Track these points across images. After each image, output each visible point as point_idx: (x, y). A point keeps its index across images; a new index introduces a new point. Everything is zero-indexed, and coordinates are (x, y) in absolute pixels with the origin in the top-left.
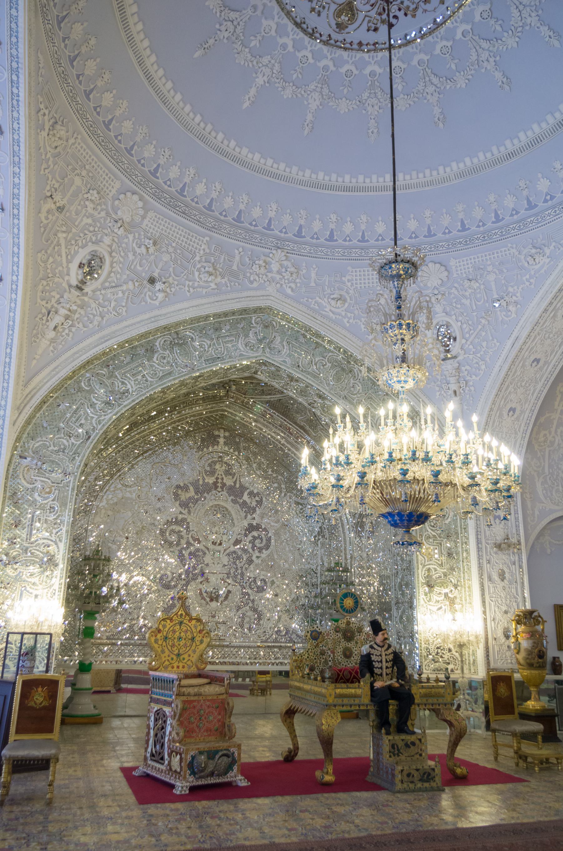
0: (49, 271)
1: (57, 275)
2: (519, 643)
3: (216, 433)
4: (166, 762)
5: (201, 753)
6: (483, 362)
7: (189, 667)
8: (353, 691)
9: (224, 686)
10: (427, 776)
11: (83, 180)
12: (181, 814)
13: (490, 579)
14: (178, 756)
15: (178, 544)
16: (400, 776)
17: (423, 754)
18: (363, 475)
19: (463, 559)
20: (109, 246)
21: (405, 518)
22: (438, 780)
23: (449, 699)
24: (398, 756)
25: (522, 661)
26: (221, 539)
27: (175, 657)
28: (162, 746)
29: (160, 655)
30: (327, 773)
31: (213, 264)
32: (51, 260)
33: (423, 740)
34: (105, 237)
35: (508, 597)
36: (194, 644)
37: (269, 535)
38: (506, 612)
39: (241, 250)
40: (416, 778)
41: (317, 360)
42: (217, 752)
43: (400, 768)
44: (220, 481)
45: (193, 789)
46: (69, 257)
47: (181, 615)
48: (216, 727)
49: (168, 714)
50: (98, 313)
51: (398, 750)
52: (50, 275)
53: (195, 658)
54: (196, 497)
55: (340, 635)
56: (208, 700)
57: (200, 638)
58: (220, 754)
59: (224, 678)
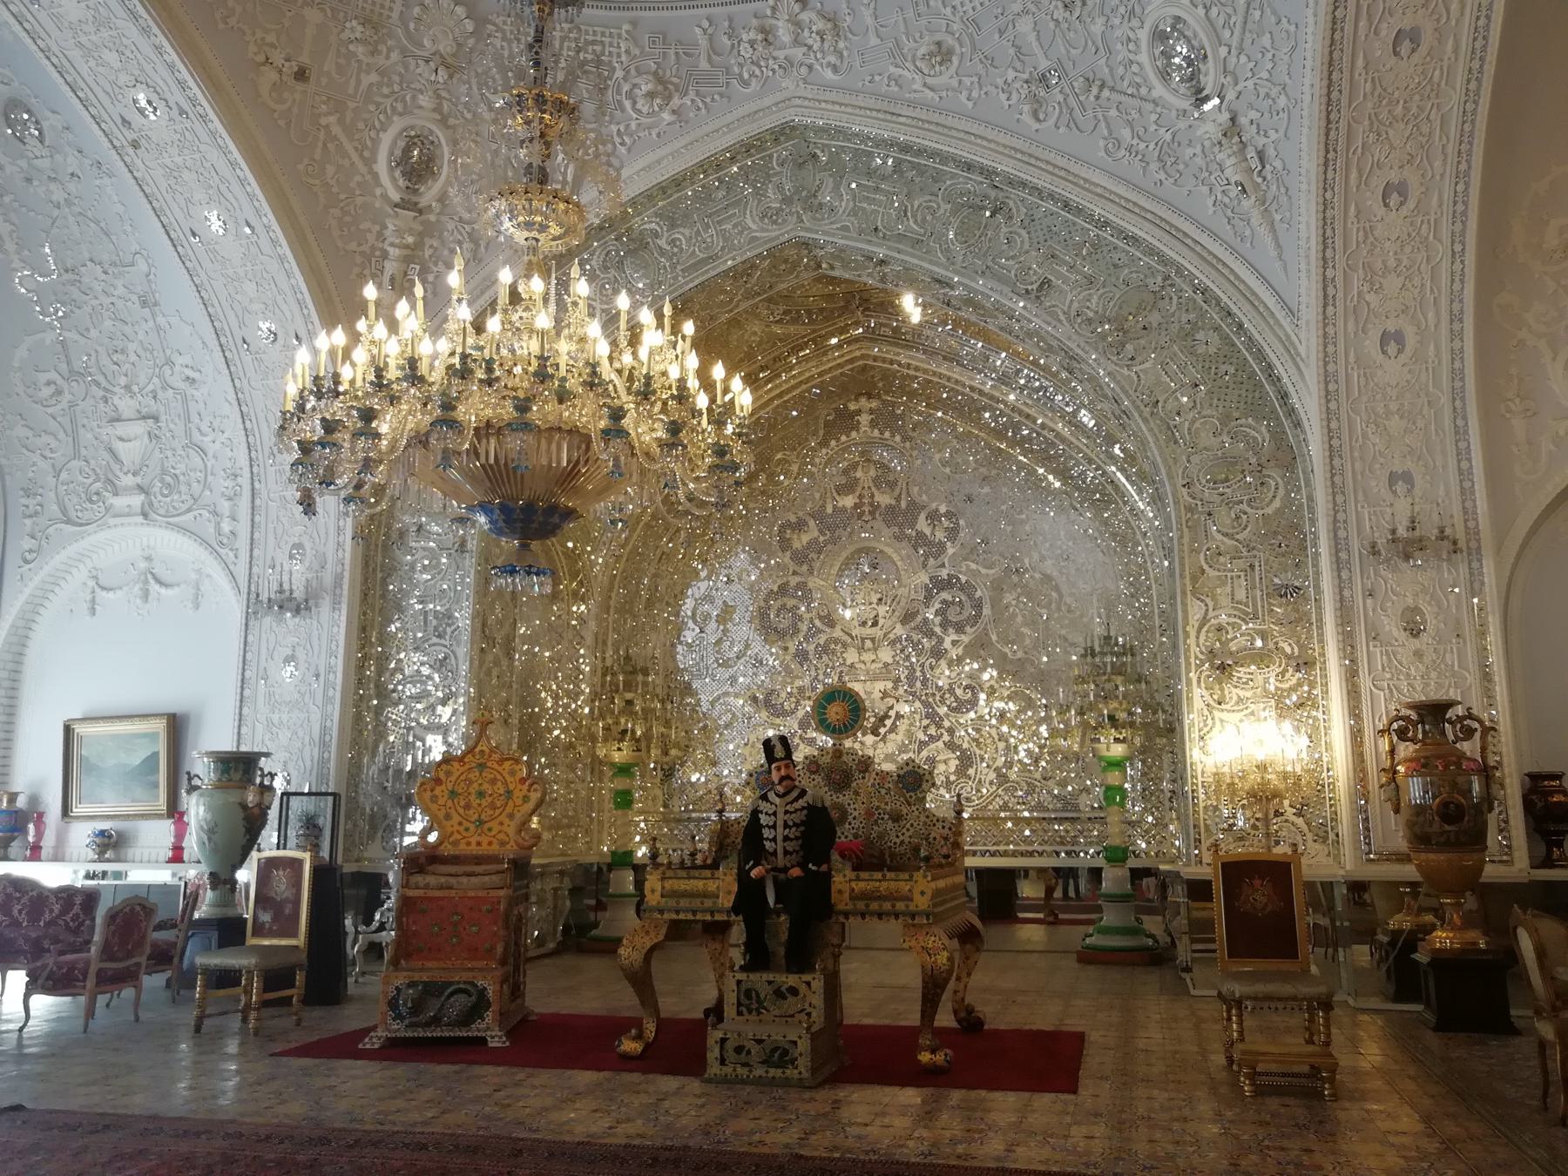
0: (335, 190)
1: (358, 192)
2: (1397, 786)
3: (852, 407)
5: (409, 985)
6: (1280, 88)
7: (503, 844)
8: (700, 884)
10: (780, 1056)
11: (323, 10)
13: (1374, 636)
17: (814, 1014)
20: (434, 110)
22: (803, 1067)
23: (922, 907)
24: (759, 1013)
26: (875, 613)
30: (639, 1037)
31: (655, 74)
32: (330, 170)
34: (421, 97)
35: (1434, 675)
36: (511, 803)
37: (978, 594)
39: (706, 24)
40: (755, 1057)
41: (916, 204)
42: (451, 983)
46: (366, 154)
48: (487, 946)
50: (466, 236)
52: (342, 196)
54: (822, 539)
57: (525, 792)
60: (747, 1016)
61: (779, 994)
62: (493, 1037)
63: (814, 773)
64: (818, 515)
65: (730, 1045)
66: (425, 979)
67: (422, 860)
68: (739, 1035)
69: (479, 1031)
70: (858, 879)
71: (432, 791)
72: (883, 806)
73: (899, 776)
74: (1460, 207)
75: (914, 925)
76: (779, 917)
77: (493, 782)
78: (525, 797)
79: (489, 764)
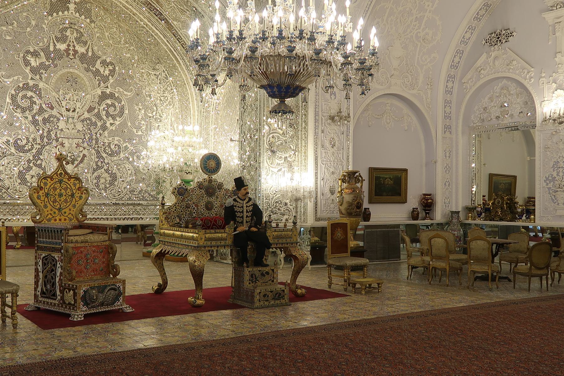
4: (59, 298)
7: (71, 220)
8: (220, 235)
9: (107, 234)
10: (278, 296)
12: (85, 333)
14: (72, 292)
15: (30, 109)
17: (275, 281)
18: (253, 50)
19: (302, 129)
21: (283, 89)
22: (287, 297)
23: (295, 240)
25: (344, 212)
27: (57, 212)
28: (54, 284)
29: (43, 210)
33: (275, 271)
35: (336, 161)
36: (74, 199)
37: (123, 103)
38: (333, 173)
42: (106, 287)
43: (258, 291)
44: (71, 48)
45: (86, 316)
49: (57, 259)
51: (256, 278)
53: (74, 211)
54: (47, 63)
55: (203, 191)
56: (94, 246)
57: (79, 195)
58: (109, 288)
59: (107, 228)
63: (201, 189)
64: (46, 50)
68: (266, 290)
69: (118, 306)
73: (232, 191)
74: (367, 9)
77: (66, 189)
79: (64, 180)
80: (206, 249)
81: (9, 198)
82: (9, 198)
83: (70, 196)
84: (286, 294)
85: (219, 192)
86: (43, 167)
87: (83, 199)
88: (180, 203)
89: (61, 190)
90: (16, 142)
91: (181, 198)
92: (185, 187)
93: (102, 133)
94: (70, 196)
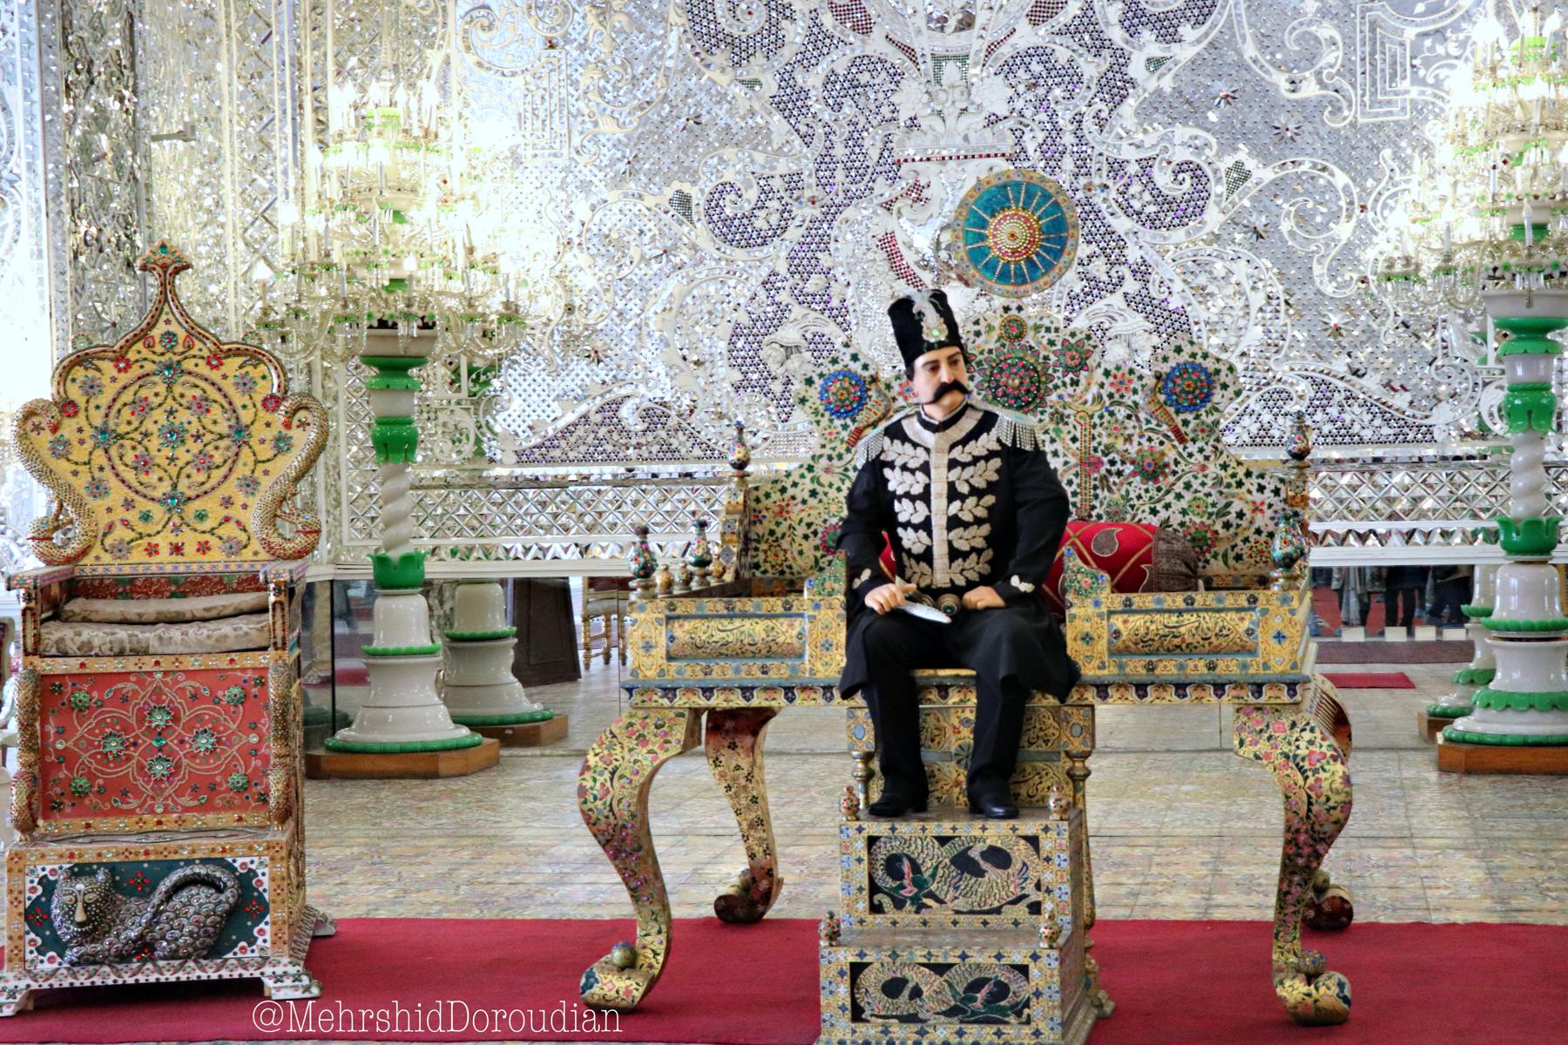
7: (234, 548)
16: (843, 990)
17: (1048, 906)
24: (920, 907)
27: (158, 511)
30: (630, 964)
36: (245, 450)
42: (172, 866)
43: (846, 956)
47: (170, 337)
48: (237, 778)
57: (278, 427)
58: (175, 877)
60: (891, 913)
61: (965, 864)
62: (278, 979)
65: (872, 980)
66: (109, 857)
67: (55, 590)
68: (894, 955)
70: (1128, 609)
71: (55, 429)
72: (1120, 444)
73: (1158, 377)
75: (1259, 709)
76: (945, 696)
77: (202, 405)
78: (279, 439)
79: (188, 365)
80: (681, 701)
81: (697, 452)
82: (697, 452)
83: (221, 437)
84: (1038, 994)
85: (1070, 390)
86: (835, 303)
87: (295, 452)
88: (840, 457)
89: (171, 412)
90: (713, 204)
91: (845, 427)
92: (865, 367)
93: (1104, 115)
94: (221, 437)
